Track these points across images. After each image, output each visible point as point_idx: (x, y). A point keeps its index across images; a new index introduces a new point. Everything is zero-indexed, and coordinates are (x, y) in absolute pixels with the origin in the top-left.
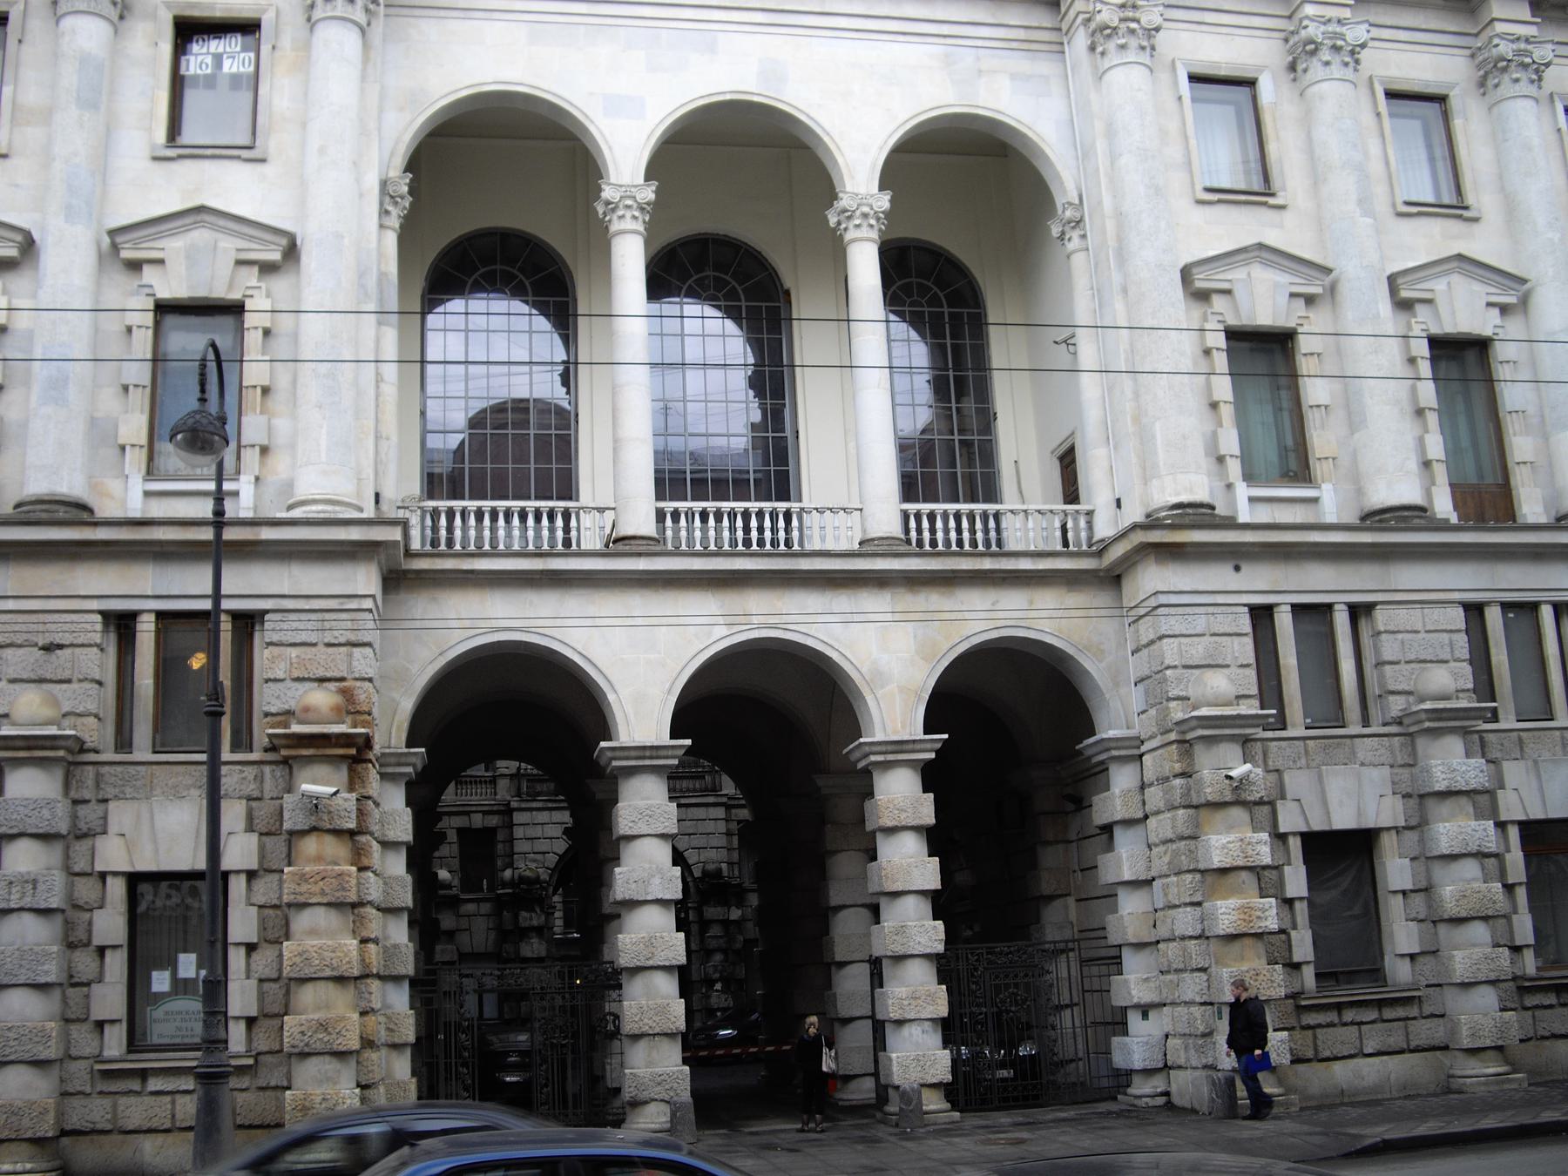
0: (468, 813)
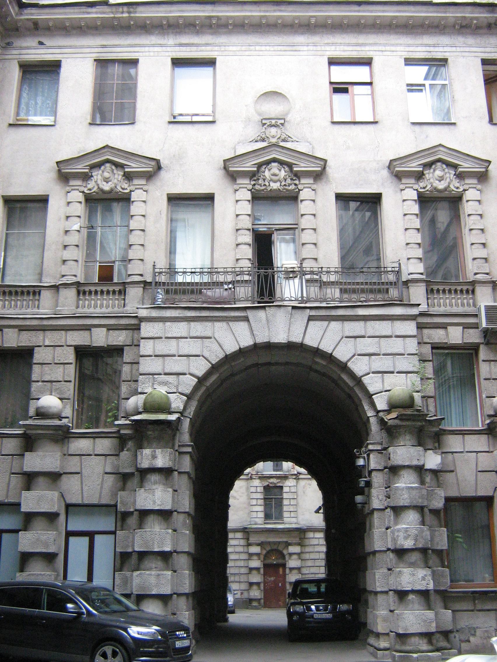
0: (88, 328)
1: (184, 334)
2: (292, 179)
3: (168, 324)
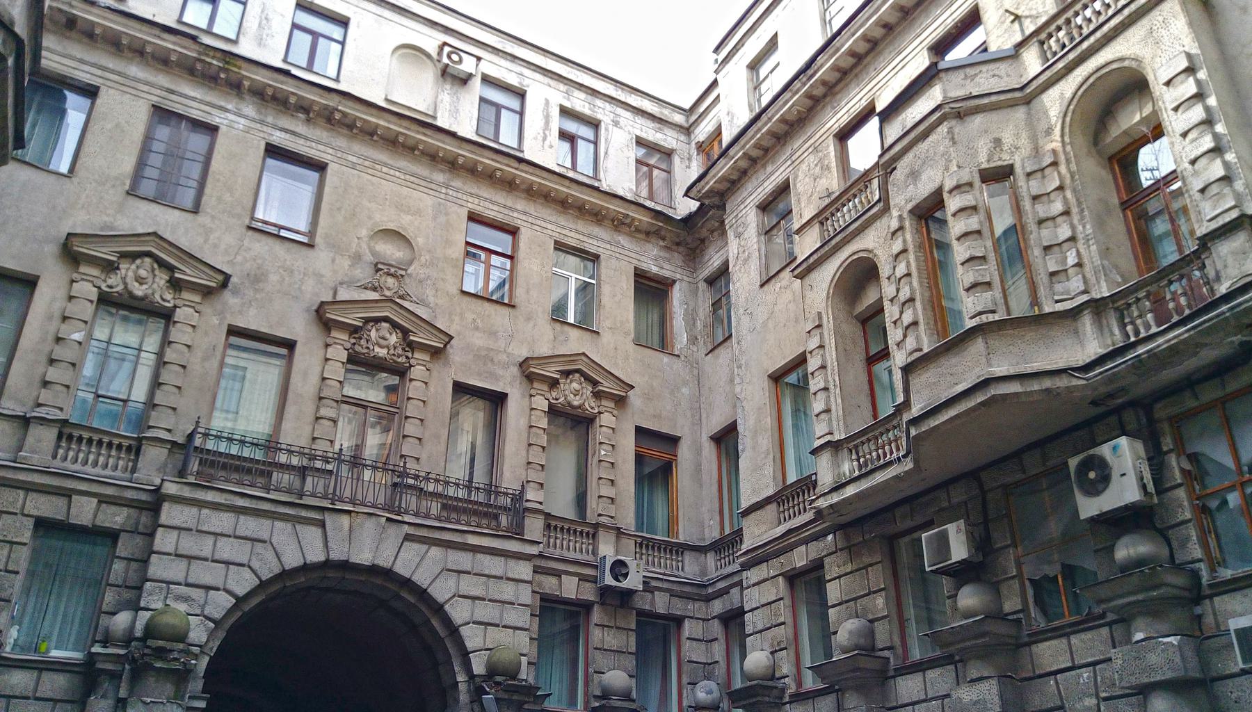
0: (67, 494)
1: (225, 531)
2: (403, 349)
3: (205, 511)
